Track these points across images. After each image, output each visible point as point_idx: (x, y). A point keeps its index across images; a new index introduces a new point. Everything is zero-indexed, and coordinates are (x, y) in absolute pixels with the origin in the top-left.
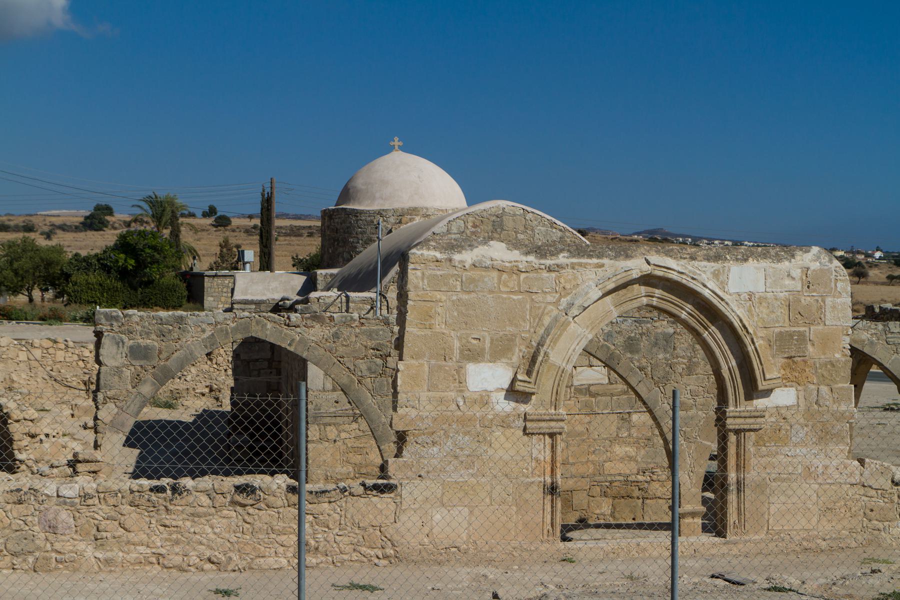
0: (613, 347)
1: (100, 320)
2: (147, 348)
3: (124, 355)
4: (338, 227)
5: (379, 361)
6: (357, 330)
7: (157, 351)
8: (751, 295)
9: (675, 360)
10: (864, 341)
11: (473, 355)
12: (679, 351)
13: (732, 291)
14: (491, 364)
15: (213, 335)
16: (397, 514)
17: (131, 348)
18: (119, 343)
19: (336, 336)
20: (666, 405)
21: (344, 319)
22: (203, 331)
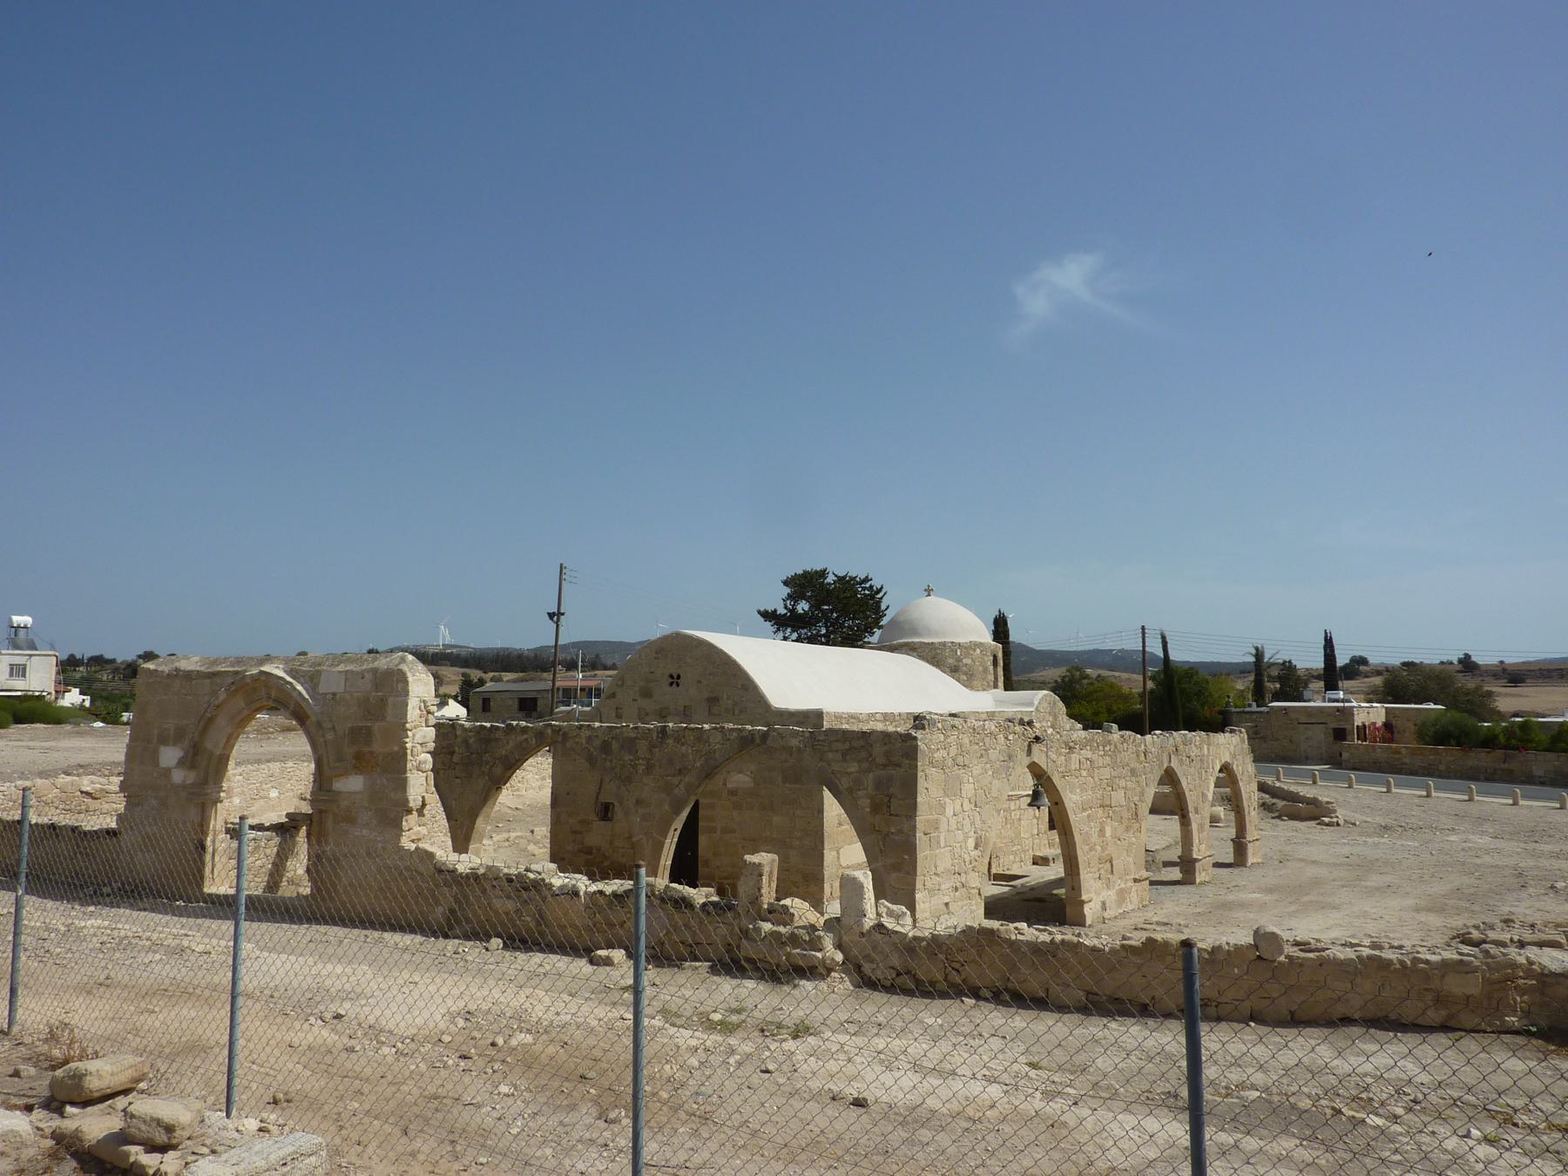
5: (449, 757)
8: (334, 694)
9: (637, 762)
10: (793, 748)
11: (163, 740)
13: (321, 692)
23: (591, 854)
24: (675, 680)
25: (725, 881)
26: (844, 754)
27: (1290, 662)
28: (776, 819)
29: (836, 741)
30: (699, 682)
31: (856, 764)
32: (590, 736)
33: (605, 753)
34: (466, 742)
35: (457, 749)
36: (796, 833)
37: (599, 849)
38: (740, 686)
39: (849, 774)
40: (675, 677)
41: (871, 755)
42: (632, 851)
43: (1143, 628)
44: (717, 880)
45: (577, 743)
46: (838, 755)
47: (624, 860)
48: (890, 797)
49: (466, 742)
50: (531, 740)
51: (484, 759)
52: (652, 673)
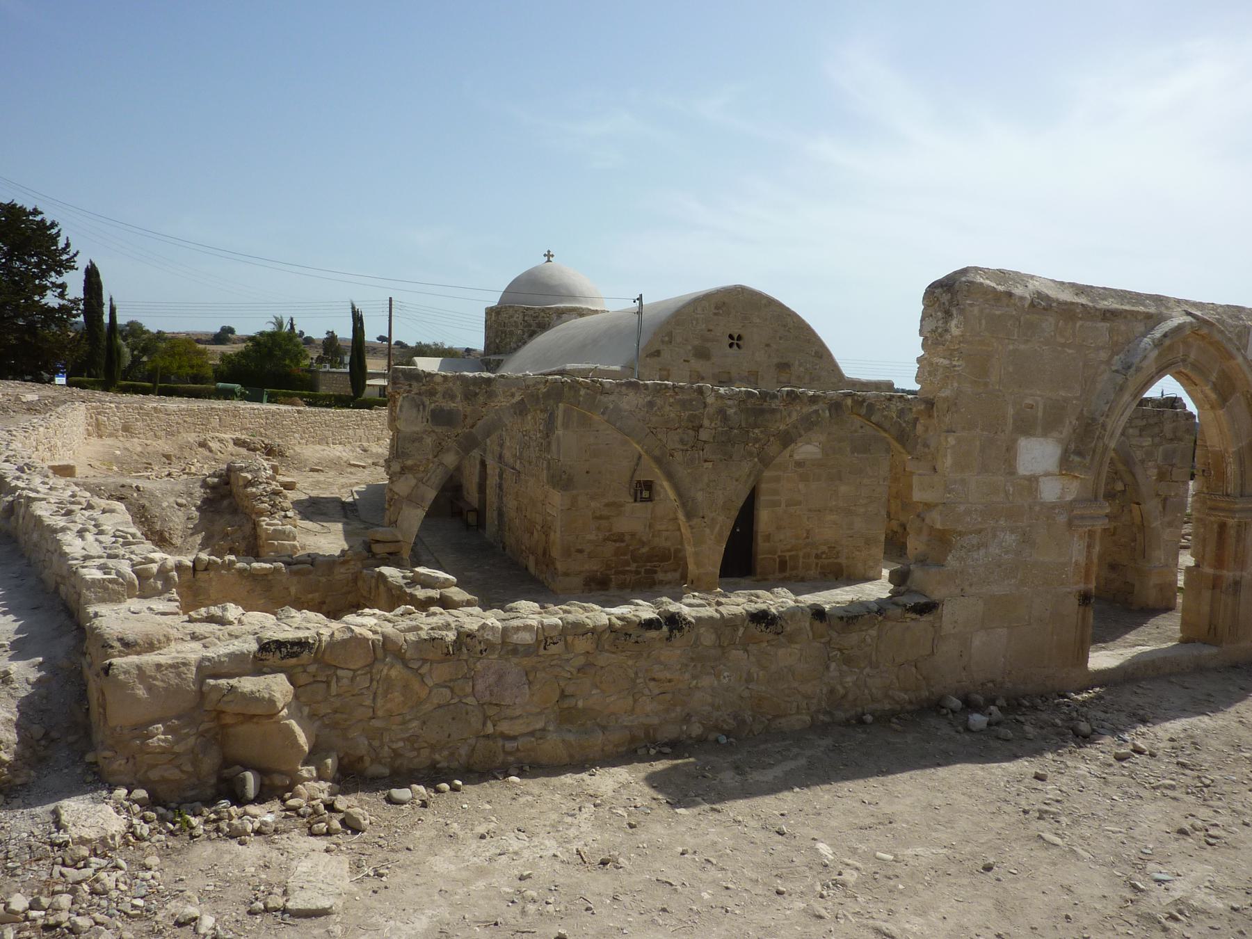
0: (904, 425)
2: (450, 412)
3: (425, 420)
4: (506, 321)
5: (690, 432)
6: (672, 400)
7: (462, 417)
11: (1025, 427)
14: (1042, 439)
15: (522, 400)
16: (936, 642)
18: (419, 406)
19: (651, 404)
22: (513, 395)
23: (623, 541)
24: (736, 342)
25: (788, 554)
26: (1142, 430)
27: (332, 332)
28: (843, 489)
29: (1136, 418)
30: (768, 345)
31: (1150, 439)
32: (903, 408)
34: (722, 412)
35: (706, 423)
36: (861, 501)
37: (633, 535)
38: (813, 354)
39: (1143, 447)
40: (736, 337)
41: (1162, 431)
42: (678, 533)
43: (391, 298)
44: (779, 554)
45: (886, 417)
46: (1137, 432)
47: (668, 544)
48: (1173, 465)
49: (722, 412)
50: (823, 411)
51: (751, 434)
52: (709, 330)
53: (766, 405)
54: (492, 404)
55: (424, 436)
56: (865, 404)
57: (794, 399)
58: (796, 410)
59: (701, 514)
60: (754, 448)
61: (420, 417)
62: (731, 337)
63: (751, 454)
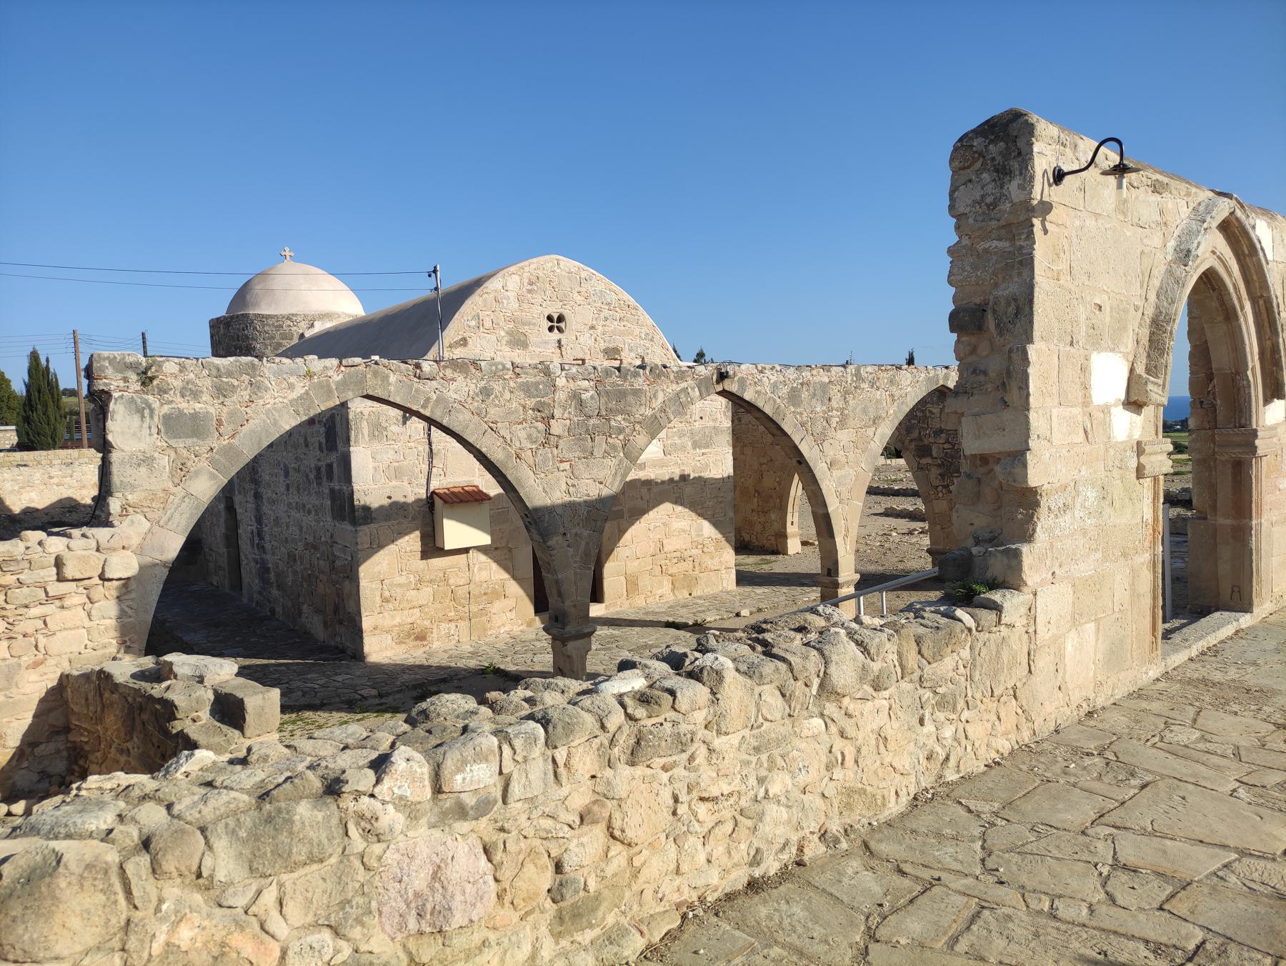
1: (103, 372)
2: (195, 416)
3: (154, 430)
5: (541, 426)
7: (214, 422)
11: (1096, 340)
12: (834, 403)
15: (307, 393)
17: (167, 419)
18: (142, 410)
19: (486, 392)
20: (824, 464)
21: (494, 368)
30: (592, 327)
32: (775, 383)
33: (794, 405)
34: (576, 396)
35: (557, 413)
45: (758, 392)
50: (693, 389)
51: (613, 423)
53: (627, 386)
54: (261, 402)
55: (156, 455)
56: (736, 379)
57: (659, 376)
58: (663, 390)
59: (562, 530)
60: (617, 441)
61: (146, 425)
62: (550, 318)
63: (614, 447)
